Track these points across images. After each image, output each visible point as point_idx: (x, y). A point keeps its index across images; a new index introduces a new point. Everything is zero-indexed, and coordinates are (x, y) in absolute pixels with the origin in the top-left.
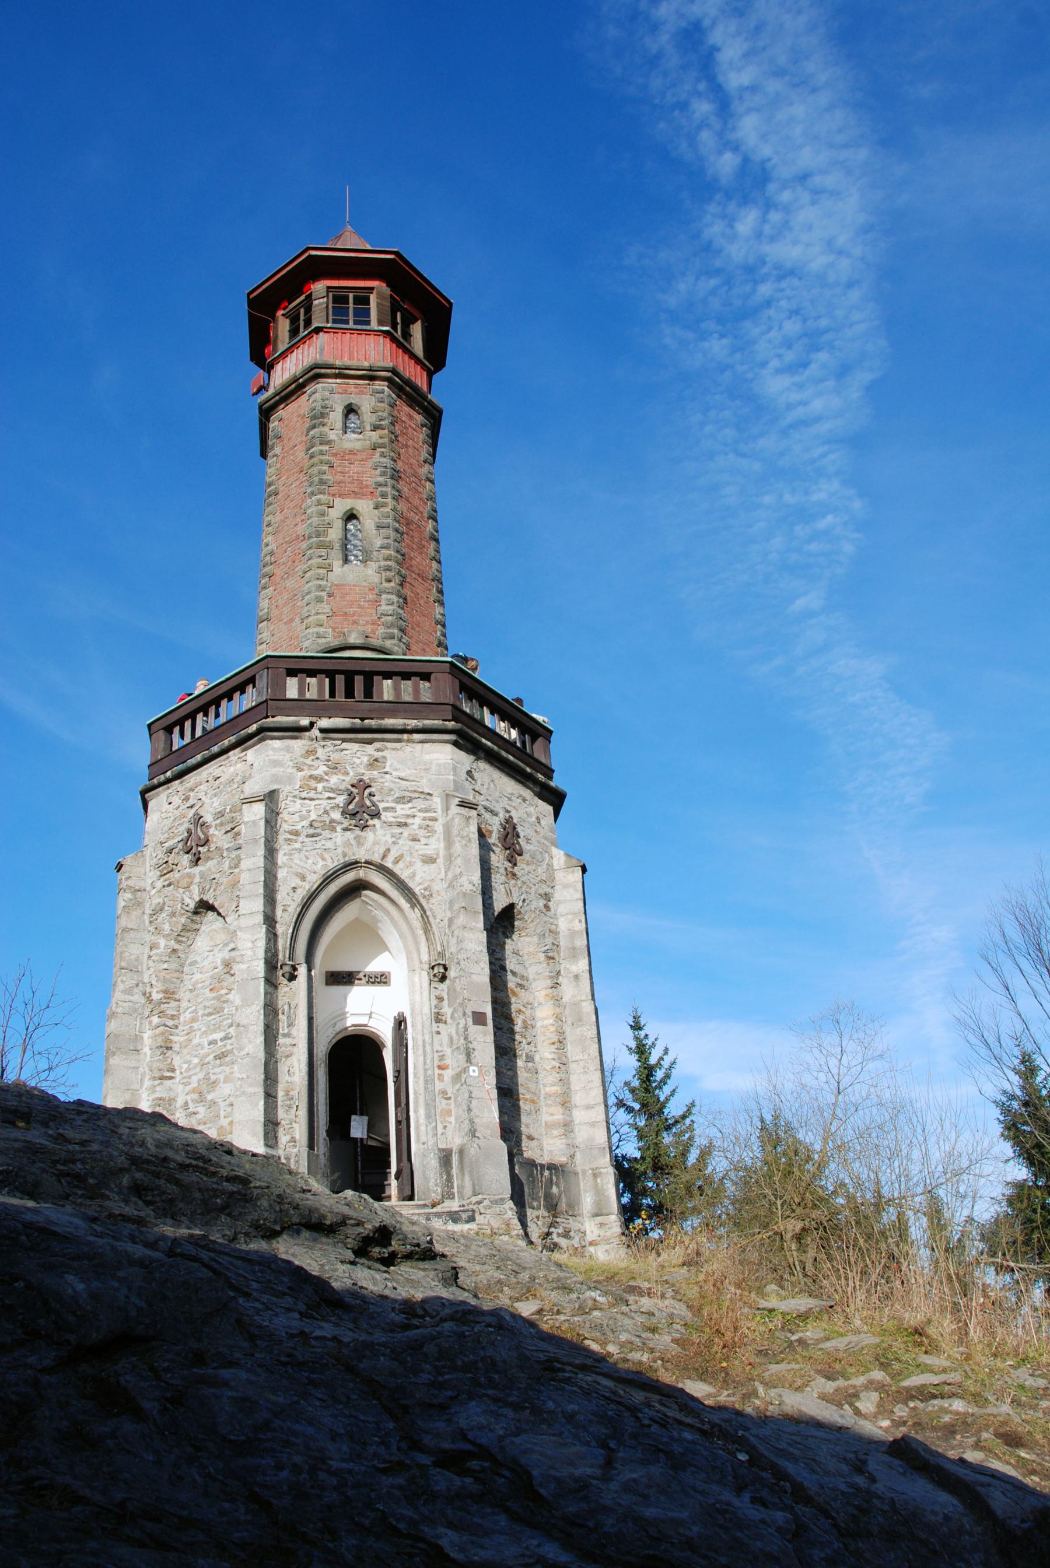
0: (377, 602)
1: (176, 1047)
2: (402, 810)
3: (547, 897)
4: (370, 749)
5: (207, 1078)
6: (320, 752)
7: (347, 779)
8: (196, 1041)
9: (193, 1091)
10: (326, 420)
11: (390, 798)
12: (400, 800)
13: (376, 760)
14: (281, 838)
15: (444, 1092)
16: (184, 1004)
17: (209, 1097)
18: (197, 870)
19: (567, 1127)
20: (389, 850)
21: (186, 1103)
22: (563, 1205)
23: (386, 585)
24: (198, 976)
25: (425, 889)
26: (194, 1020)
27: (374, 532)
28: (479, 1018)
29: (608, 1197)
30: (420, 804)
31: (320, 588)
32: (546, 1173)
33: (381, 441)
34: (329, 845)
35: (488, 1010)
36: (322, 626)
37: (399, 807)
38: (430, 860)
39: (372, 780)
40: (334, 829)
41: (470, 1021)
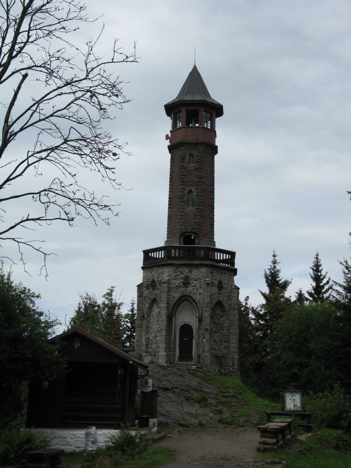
1: (150, 327)
2: (195, 282)
3: (229, 296)
5: (155, 335)
8: (153, 327)
10: (184, 160)
11: (193, 280)
12: (195, 280)
13: (191, 271)
17: (156, 339)
21: (152, 339)
24: (154, 313)
25: (199, 301)
26: (153, 322)
27: (196, 197)
30: (199, 281)
32: (221, 358)
36: (181, 226)
38: (200, 294)
39: (189, 276)
41: (205, 330)
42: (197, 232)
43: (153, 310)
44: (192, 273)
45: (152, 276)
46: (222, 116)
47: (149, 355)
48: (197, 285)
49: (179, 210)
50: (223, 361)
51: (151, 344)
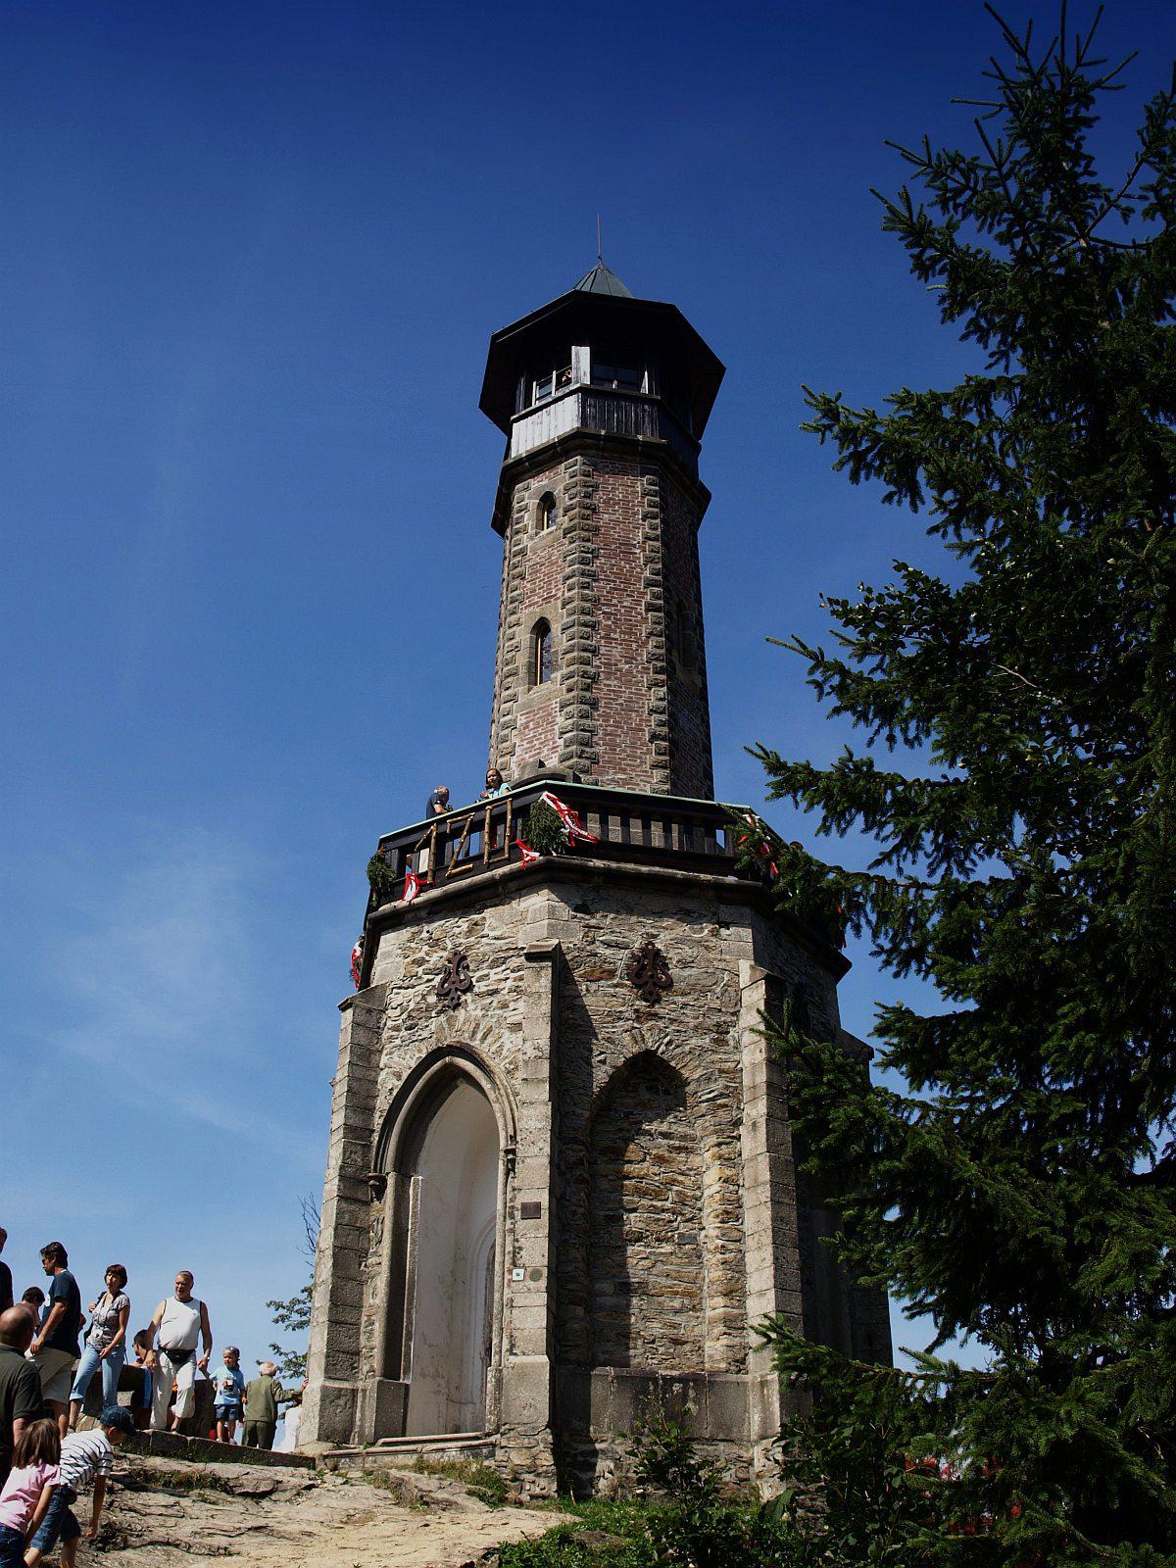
2: (495, 974)
7: (445, 954)
12: (495, 964)
20: (478, 1025)
25: (510, 1063)
29: (772, 1413)
32: (677, 1387)
38: (516, 1027)
39: (468, 948)
44: (485, 932)
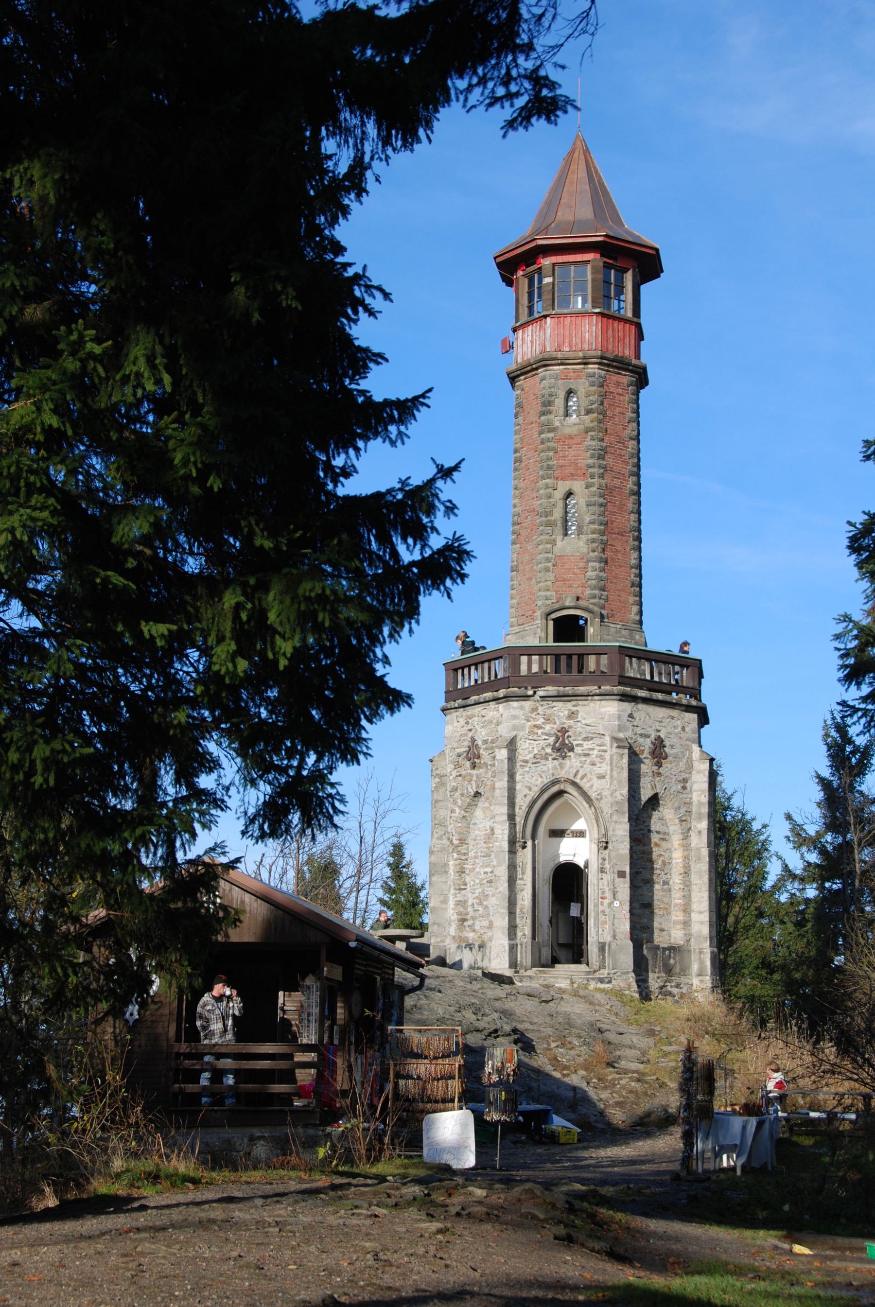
0: (585, 569)
1: (467, 871)
2: (587, 745)
3: (685, 781)
4: (569, 705)
5: (483, 892)
6: (541, 710)
7: (555, 726)
8: (477, 870)
9: (476, 898)
10: (552, 408)
12: (586, 739)
13: (573, 713)
14: (518, 765)
15: (603, 912)
16: (471, 847)
17: (485, 903)
18: (474, 772)
19: (686, 924)
20: (578, 771)
22: (677, 969)
23: (592, 554)
26: (476, 857)
27: (585, 509)
28: (621, 874)
29: (706, 966)
30: (597, 741)
31: (548, 560)
32: (667, 952)
33: (591, 425)
34: (545, 768)
35: (627, 869)
36: (548, 590)
37: (585, 743)
38: (601, 777)
39: (570, 727)
40: (547, 759)
41: (616, 876)
42: (591, 607)
43: (475, 824)
45: (470, 730)
46: (659, 276)
47: (468, 949)
48: (591, 752)
49: (540, 547)
50: (672, 961)
51: (474, 918)
